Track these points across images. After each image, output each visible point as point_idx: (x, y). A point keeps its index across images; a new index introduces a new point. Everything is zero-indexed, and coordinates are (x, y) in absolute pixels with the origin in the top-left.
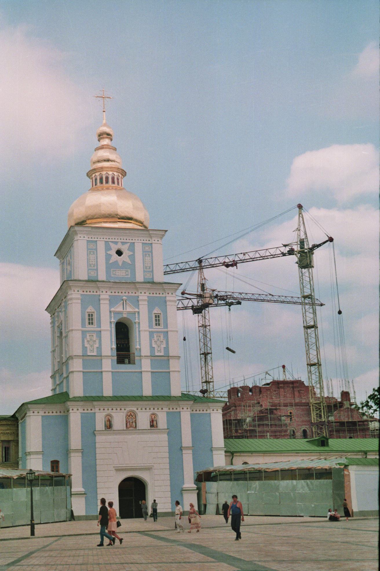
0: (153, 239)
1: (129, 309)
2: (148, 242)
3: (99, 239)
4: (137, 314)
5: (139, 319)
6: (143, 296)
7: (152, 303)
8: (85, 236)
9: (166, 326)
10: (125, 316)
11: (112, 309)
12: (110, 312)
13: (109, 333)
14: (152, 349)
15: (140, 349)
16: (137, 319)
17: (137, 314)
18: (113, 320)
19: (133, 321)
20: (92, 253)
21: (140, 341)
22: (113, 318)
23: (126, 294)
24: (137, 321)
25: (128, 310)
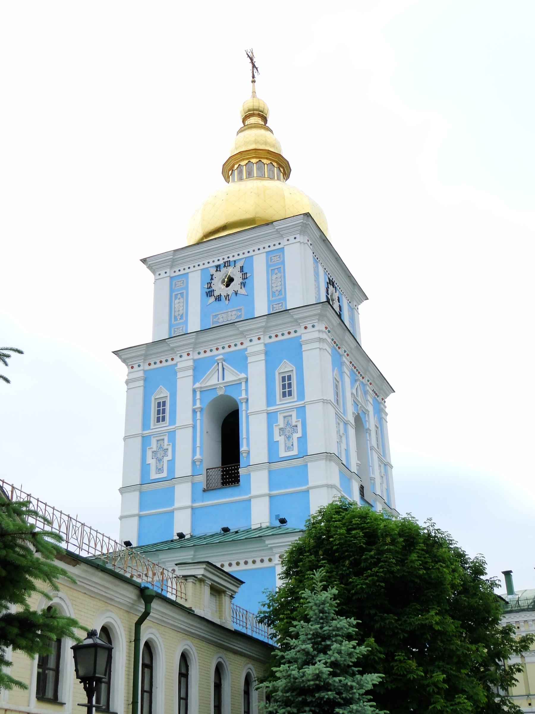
0: (286, 239)
1: (230, 377)
2: (278, 247)
3: (192, 269)
4: (243, 384)
5: (247, 390)
6: (255, 348)
7: (271, 356)
8: (168, 270)
9: (302, 395)
10: (221, 393)
11: (197, 385)
12: (194, 391)
13: (190, 430)
14: (272, 446)
15: (248, 453)
16: (244, 392)
17: (243, 384)
18: (198, 405)
19: (238, 398)
20: (179, 296)
21: (248, 438)
22: (198, 402)
23: (221, 351)
24: (244, 396)
25: (226, 380)
